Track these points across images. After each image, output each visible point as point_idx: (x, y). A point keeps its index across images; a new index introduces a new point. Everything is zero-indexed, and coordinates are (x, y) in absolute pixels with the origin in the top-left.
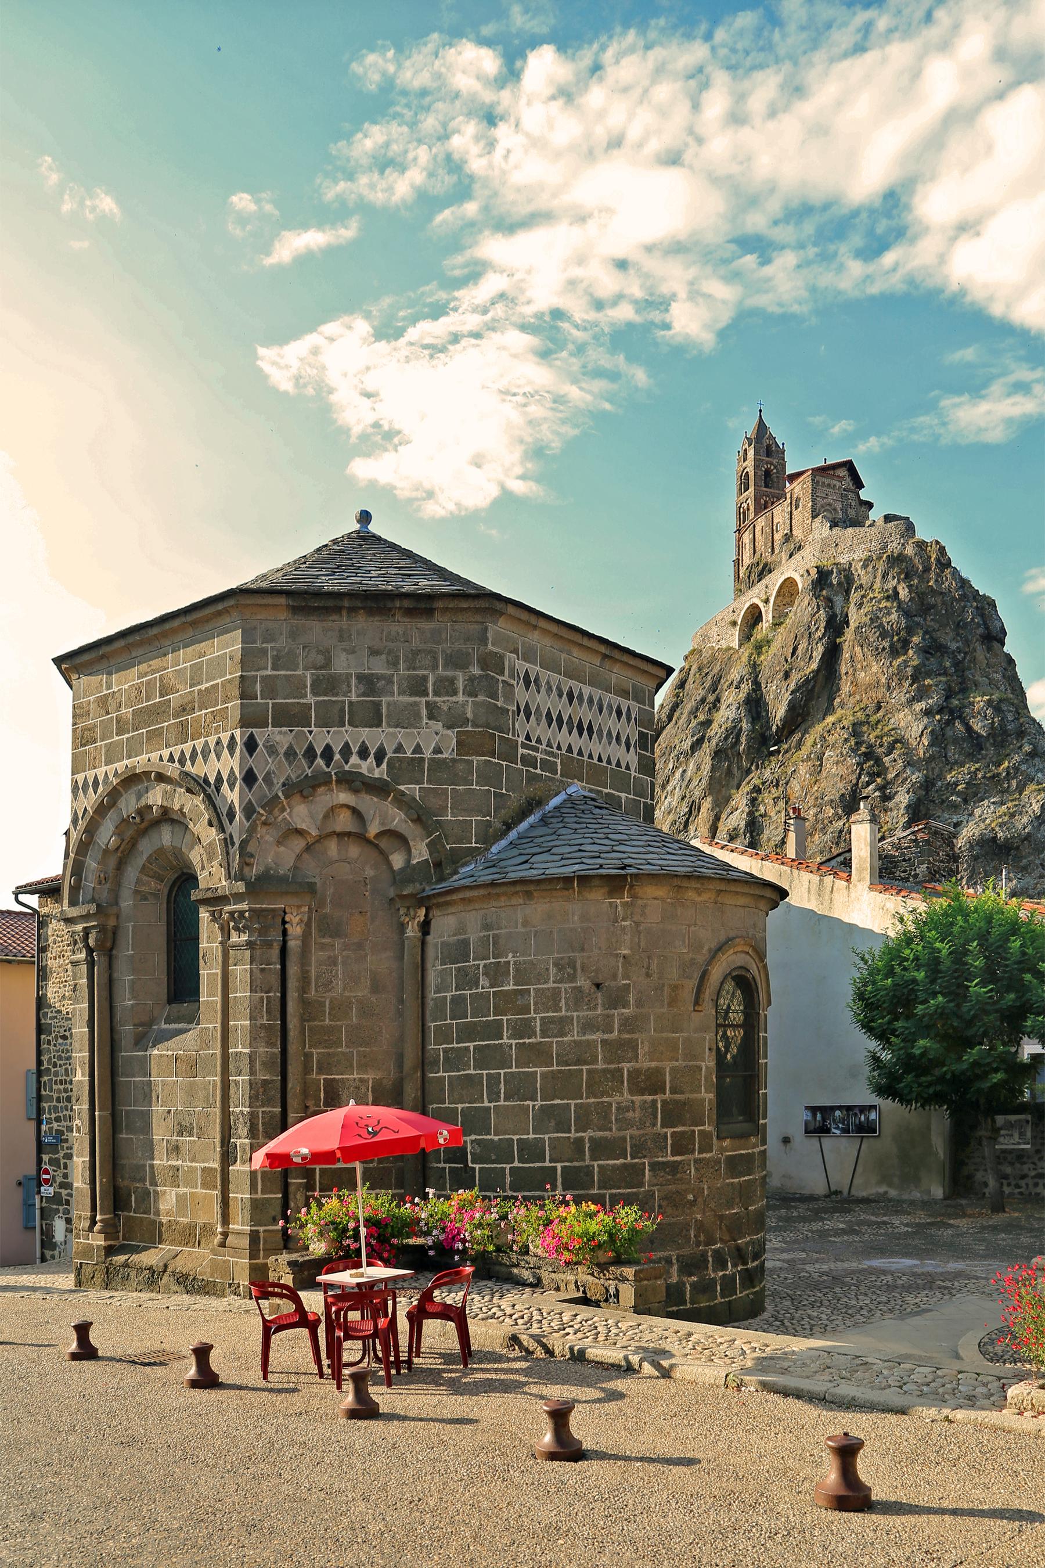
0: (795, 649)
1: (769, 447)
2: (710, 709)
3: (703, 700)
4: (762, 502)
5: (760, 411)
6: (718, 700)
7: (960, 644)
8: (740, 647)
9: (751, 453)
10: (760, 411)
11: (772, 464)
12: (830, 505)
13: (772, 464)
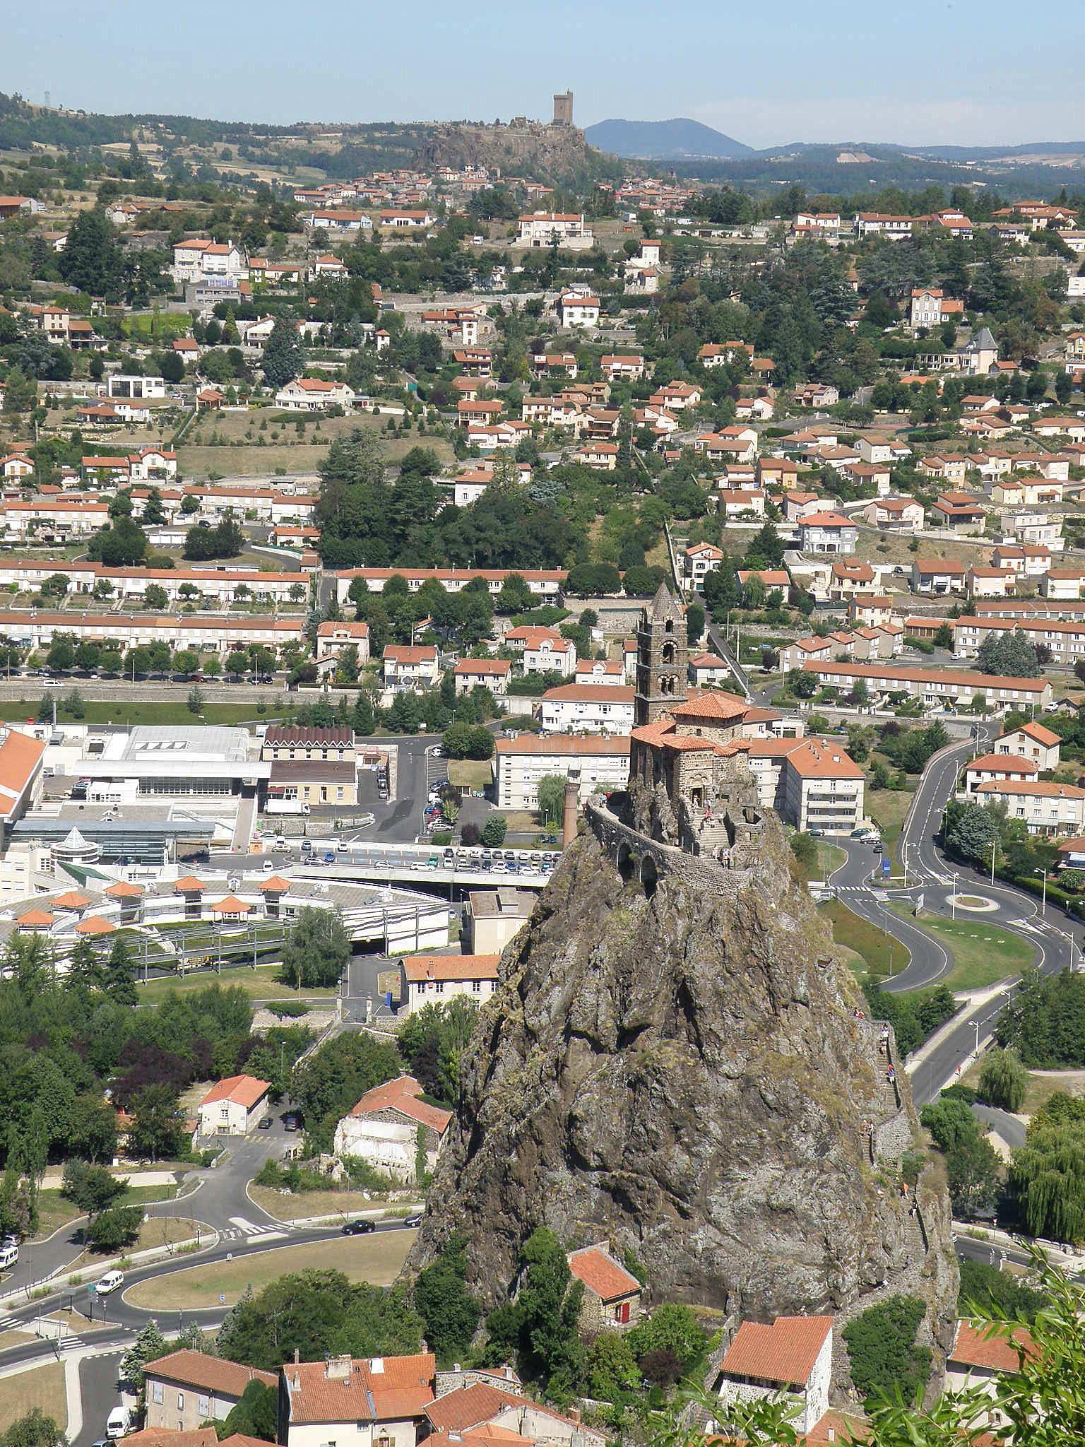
4: (660, 681)
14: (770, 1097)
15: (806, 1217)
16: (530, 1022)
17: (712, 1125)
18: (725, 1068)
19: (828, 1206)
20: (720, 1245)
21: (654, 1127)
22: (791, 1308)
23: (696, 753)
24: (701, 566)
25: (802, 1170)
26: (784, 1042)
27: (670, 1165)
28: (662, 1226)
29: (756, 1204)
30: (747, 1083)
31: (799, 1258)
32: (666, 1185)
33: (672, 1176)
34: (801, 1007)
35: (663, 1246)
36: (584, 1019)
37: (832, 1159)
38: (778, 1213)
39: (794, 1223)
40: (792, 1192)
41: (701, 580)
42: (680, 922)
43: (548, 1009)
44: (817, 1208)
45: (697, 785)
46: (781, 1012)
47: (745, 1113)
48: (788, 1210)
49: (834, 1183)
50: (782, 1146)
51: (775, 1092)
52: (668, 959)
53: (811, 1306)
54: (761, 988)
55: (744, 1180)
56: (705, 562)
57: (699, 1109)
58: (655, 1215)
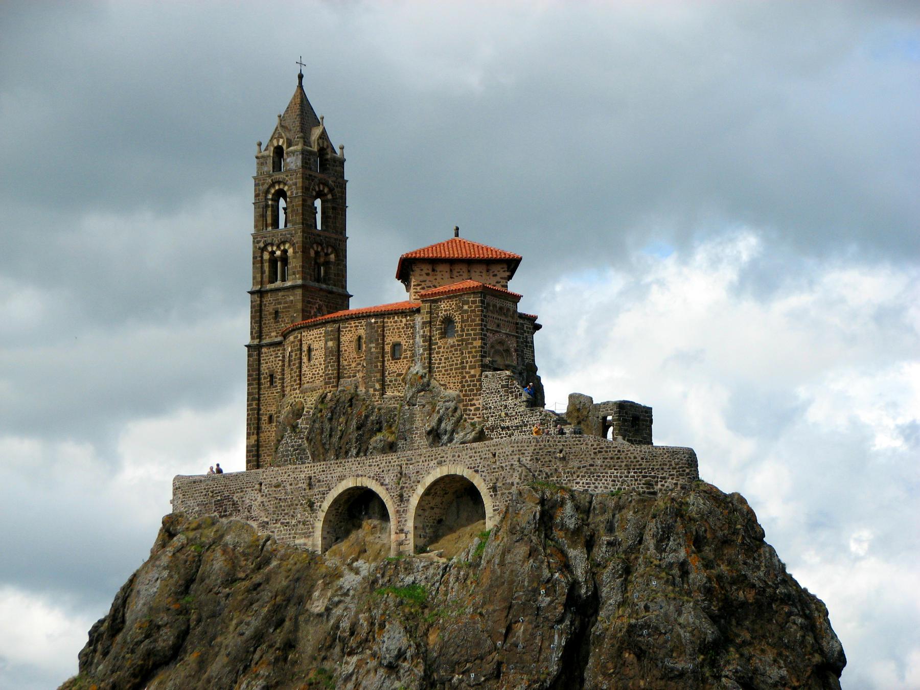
0: (509, 629)
1: (322, 151)
2: (277, 660)
3: (258, 638)
4: (312, 253)
5: (301, 77)
6: (290, 645)
7: (784, 672)
8: (325, 550)
9: (293, 162)
10: (301, 77)
11: (325, 184)
12: (501, 343)
13: (325, 184)
52: (569, 616)
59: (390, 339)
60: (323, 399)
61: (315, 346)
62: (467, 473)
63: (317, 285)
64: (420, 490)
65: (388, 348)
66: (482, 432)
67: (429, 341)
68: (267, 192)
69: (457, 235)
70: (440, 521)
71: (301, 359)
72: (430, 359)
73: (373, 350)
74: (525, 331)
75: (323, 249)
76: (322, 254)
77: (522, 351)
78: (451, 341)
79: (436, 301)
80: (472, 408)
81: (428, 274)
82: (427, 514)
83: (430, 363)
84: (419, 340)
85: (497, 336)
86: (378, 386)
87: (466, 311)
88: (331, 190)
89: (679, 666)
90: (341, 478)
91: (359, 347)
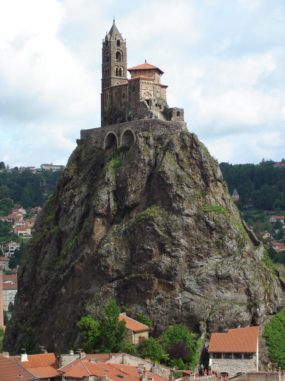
1: (118, 41)
4: (115, 69)
13: (119, 50)
14: (212, 223)
15: (237, 281)
16: (63, 229)
17: (182, 241)
18: (186, 211)
19: (248, 273)
20: (192, 300)
21: (149, 247)
22: (234, 325)
23: (146, 81)
24: (12, 248)
25: (232, 257)
26: (213, 200)
27: (161, 264)
28: (158, 297)
29: (210, 276)
30: (198, 218)
31: (234, 301)
32: (158, 274)
33: (163, 269)
34: (219, 183)
35: (159, 307)
36: (103, 207)
37: (247, 250)
38: (221, 279)
39: (231, 284)
40: (228, 268)
41: (13, 253)
42: (151, 151)
43: (74, 220)
44: (242, 275)
45: (147, 98)
46: (211, 185)
47: (198, 233)
48: (228, 278)
49: (249, 262)
50: (220, 246)
51: (214, 221)
53: (243, 324)
54: (198, 175)
55: (202, 266)
56: (14, 246)
57: (173, 234)
58: (153, 292)
59: (123, 92)
60: (109, 108)
61: (109, 94)
62: (131, 129)
63: (117, 77)
64: (123, 134)
65: (122, 95)
66: (140, 117)
67: (129, 92)
68: (105, 53)
69: (146, 62)
70: (131, 142)
71: (106, 98)
72: (130, 98)
73: (119, 95)
74: (157, 89)
75: (119, 67)
76: (119, 69)
77: (156, 94)
78: (134, 93)
79: (131, 82)
80: (138, 111)
81: (135, 74)
82: (126, 140)
83: (130, 99)
84: (128, 93)
85: (146, 91)
86: (120, 105)
87: (136, 85)
88: (121, 51)
89: (171, 182)
90: (108, 131)
91: (116, 95)
